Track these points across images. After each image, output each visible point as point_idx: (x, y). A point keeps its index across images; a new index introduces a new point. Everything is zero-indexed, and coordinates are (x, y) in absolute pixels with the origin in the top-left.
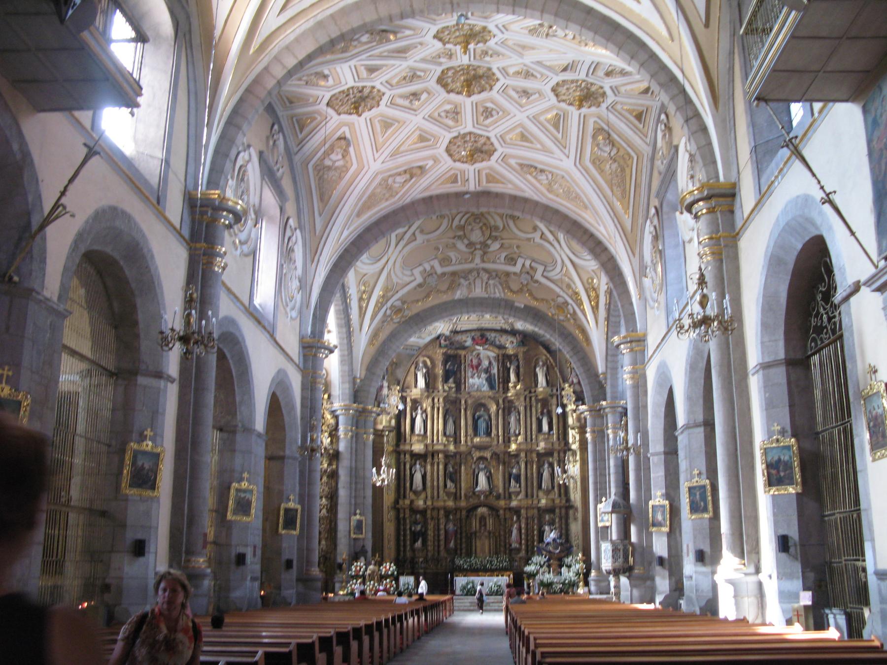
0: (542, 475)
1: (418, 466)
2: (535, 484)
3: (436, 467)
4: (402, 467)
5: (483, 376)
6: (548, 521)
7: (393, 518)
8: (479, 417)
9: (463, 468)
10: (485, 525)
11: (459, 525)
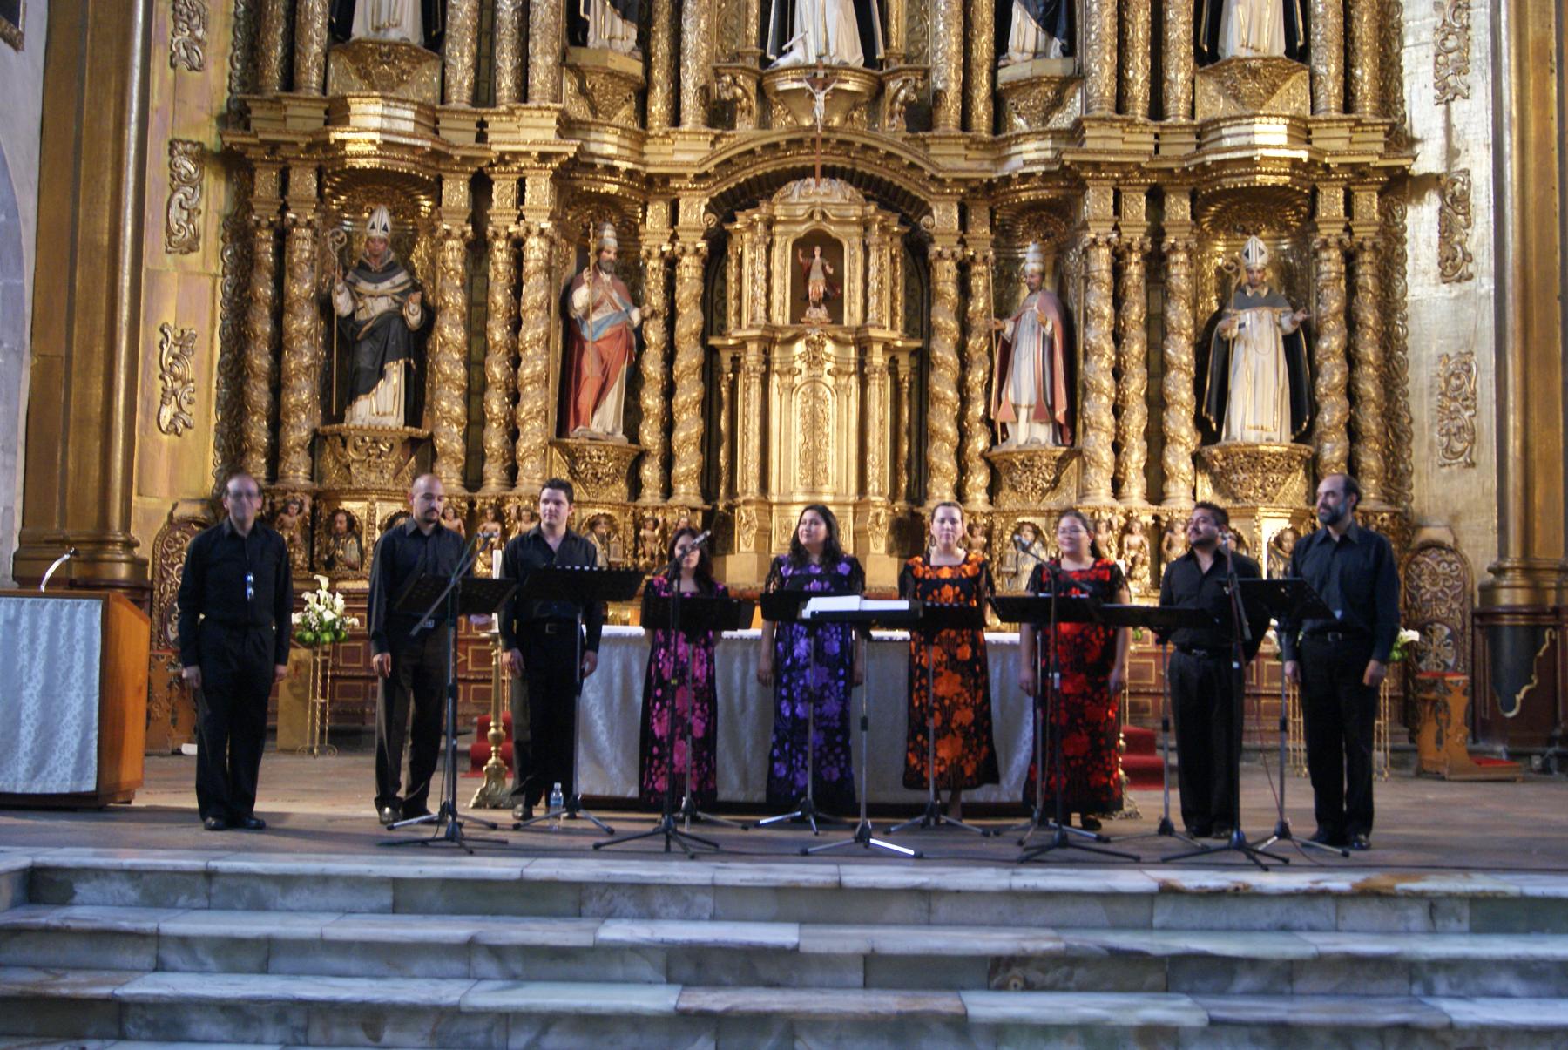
7: (210, 225)
10: (833, 300)
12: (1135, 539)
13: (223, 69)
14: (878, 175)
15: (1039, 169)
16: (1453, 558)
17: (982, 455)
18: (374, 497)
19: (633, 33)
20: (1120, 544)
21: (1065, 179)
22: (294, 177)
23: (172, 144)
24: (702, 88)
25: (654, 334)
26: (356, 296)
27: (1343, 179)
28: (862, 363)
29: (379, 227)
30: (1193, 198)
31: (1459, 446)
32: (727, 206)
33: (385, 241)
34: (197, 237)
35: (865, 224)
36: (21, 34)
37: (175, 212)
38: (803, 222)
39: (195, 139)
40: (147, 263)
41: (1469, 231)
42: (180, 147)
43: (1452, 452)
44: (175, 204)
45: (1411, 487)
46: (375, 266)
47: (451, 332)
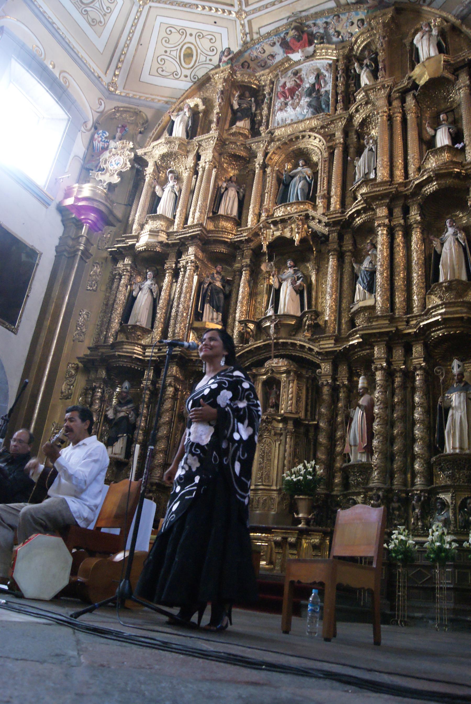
0: (438, 256)
1: (148, 282)
4: (115, 285)
5: (305, 100)
8: (292, 177)
9: (245, 276)
14: (301, 355)
26: (116, 412)
28: (285, 429)
30: (426, 347)
34: (71, 394)
35: (288, 372)
36: (17, 329)
37: (64, 385)
42: (70, 365)
46: (122, 402)
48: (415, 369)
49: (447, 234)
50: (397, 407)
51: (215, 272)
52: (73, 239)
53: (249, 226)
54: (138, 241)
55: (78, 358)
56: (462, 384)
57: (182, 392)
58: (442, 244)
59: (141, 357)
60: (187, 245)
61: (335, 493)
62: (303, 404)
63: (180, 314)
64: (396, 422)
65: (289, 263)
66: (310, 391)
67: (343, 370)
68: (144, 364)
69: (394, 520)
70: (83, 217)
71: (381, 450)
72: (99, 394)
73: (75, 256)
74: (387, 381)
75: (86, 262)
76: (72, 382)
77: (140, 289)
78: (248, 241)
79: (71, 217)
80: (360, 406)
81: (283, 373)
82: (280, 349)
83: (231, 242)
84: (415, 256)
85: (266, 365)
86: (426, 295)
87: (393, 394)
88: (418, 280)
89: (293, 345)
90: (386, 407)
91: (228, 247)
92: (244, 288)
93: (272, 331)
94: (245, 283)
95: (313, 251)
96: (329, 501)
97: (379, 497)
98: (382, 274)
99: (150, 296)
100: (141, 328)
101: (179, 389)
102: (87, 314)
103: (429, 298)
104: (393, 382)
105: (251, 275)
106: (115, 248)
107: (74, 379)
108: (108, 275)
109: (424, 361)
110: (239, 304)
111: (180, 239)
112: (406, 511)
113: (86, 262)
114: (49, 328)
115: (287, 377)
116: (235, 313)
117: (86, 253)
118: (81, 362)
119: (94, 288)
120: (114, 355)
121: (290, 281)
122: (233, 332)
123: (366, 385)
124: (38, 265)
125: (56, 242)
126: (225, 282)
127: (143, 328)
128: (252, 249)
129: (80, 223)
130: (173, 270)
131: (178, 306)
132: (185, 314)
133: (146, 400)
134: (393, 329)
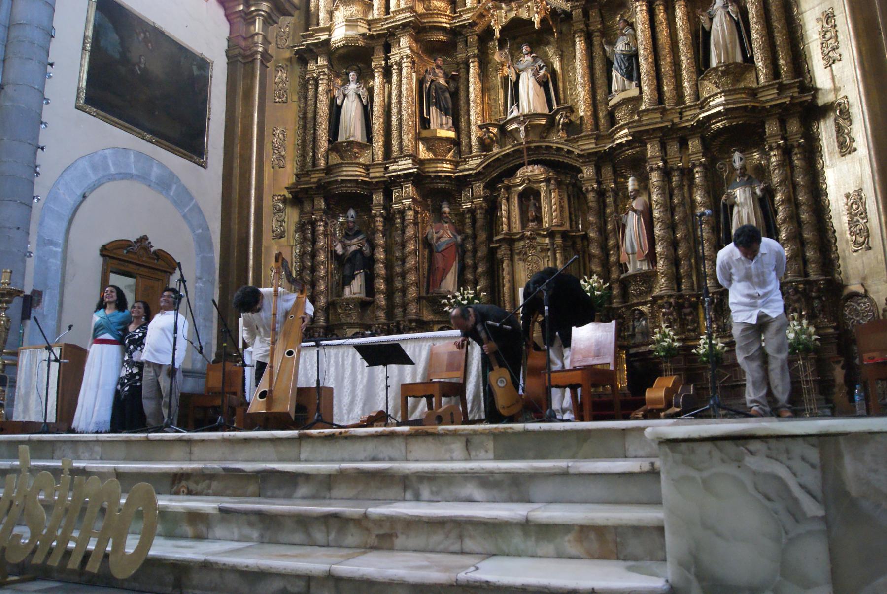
0: (707, 34)
1: (353, 86)
2: (685, 60)
3: (395, 78)
4: (311, 93)
6: (743, 168)
9: (473, 70)
10: (538, 219)
11: (469, 231)
12: (687, 310)
13: (293, 166)
15: (625, 139)
16: (866, 300)
17: (618, 280)
18: (345, 327)
19: (450, 121)
20: (679, 315)
21: (639, 143)
22: (316, 202)
23: (273, 198)
24: (478, 137)
25: (469, 247)
26: (345, 247)
27: (776, 114)
28: (553, 244)
29: (350, 216)
30: (703, 140)
31: (861, 240)
32: (491, 186)
33: (353, 222)
34: (284, 232)
35: (547, 181)
36: (206, 162)
38: (520, 185)
39: (282, 194)
40: (264, 244)
41: (851, 127)
42: (276, 198)
43: (858, 244)
44: (274, 220)
45: (839, 266)
46: (350, 233)
47: (381, 255)
48: (694, 166)
49: (715, 7)
50: (677, 209)
51: (434, 66)
52: (245, 39)
53: (468, 6)
54: (330, 35)
55: (287, 188)
56: (746, 179)
57: (422, 215)
58: (711, 20)
59: (367, 180)
60: (397, 35)
61: (615, 305)
62: (566, 214)
63: (404, 123)
64: (679, 225)
65: (525, 49)
66: (572, 199)
67: (607, 171)
68: (371, 187)
69: (688, 325)
70: (253, 9)
71: (667, 255)
72: (322, 228)
73: (254, 61)
74: (663, 181)
75: (267, 67)
76: (283, 218)
77: (345, 96)
78: (473, 24)
79: (237, 10)
80: (635, 211)
81: (542, 182)
82: (532, 155)
83: (451, 27)
84: (682, 36)
85: (519, 173)
86: (697, 81)
87: (671, 196)
88: (688, 64)
89: (548, 148)
90: (667, 210)
91: (447, 33)
92: (475, 84)
93: (522, 134)
94: (475, 77)
95: (553, 33)
96: (611, 314)
97: (670, 304)
98: (646, 59)
99: (359, 103)
100: (359, 145)
101: (418, 211)
102: (283, 132)
103: (701, 84)
104: (670, 181)
105: (480, 67)
106: (303, 45)
107: (284, 214)
108: (296, 82)
109: (703, 156)
110: (472, 104)
111: (388, 28)
112: (697, 316)
113: (267, 67)
114: (241, 155)
115: (547, 186)
116: (469, 115)
117: (266, 56)
118: (291, 193)
119: (284, 99)
120: (336, 181)
121: (530, 70)
122: (470, 138)
123: (637, 187)
124: (211, 77)
125: (225, 45)
126: (449, 78)
127: (359, 143)
128: (477, 35)
129: (249, 17)
130: (383, 68)
131: (400, 112)
132: (411, 123)
133: (381, 228)
134: (669, 124)
